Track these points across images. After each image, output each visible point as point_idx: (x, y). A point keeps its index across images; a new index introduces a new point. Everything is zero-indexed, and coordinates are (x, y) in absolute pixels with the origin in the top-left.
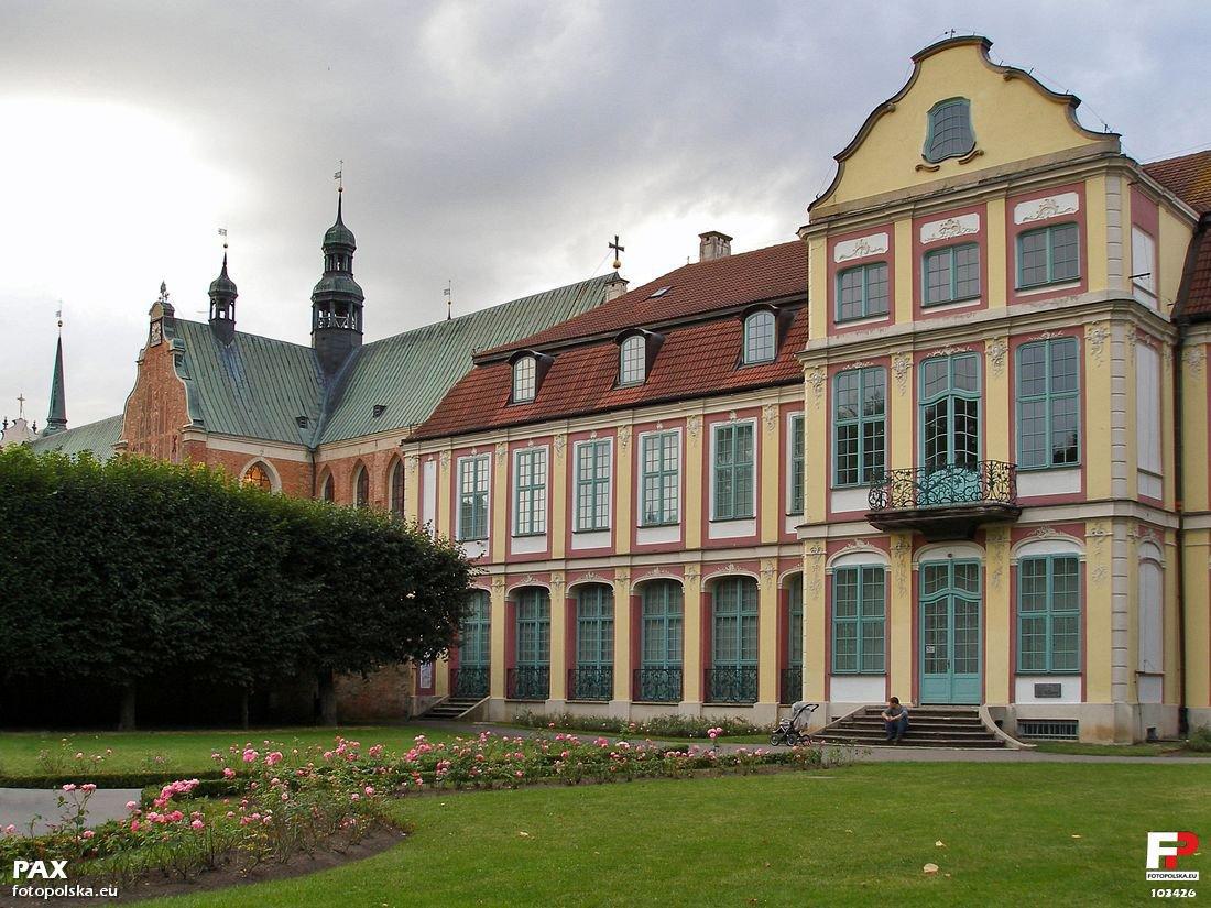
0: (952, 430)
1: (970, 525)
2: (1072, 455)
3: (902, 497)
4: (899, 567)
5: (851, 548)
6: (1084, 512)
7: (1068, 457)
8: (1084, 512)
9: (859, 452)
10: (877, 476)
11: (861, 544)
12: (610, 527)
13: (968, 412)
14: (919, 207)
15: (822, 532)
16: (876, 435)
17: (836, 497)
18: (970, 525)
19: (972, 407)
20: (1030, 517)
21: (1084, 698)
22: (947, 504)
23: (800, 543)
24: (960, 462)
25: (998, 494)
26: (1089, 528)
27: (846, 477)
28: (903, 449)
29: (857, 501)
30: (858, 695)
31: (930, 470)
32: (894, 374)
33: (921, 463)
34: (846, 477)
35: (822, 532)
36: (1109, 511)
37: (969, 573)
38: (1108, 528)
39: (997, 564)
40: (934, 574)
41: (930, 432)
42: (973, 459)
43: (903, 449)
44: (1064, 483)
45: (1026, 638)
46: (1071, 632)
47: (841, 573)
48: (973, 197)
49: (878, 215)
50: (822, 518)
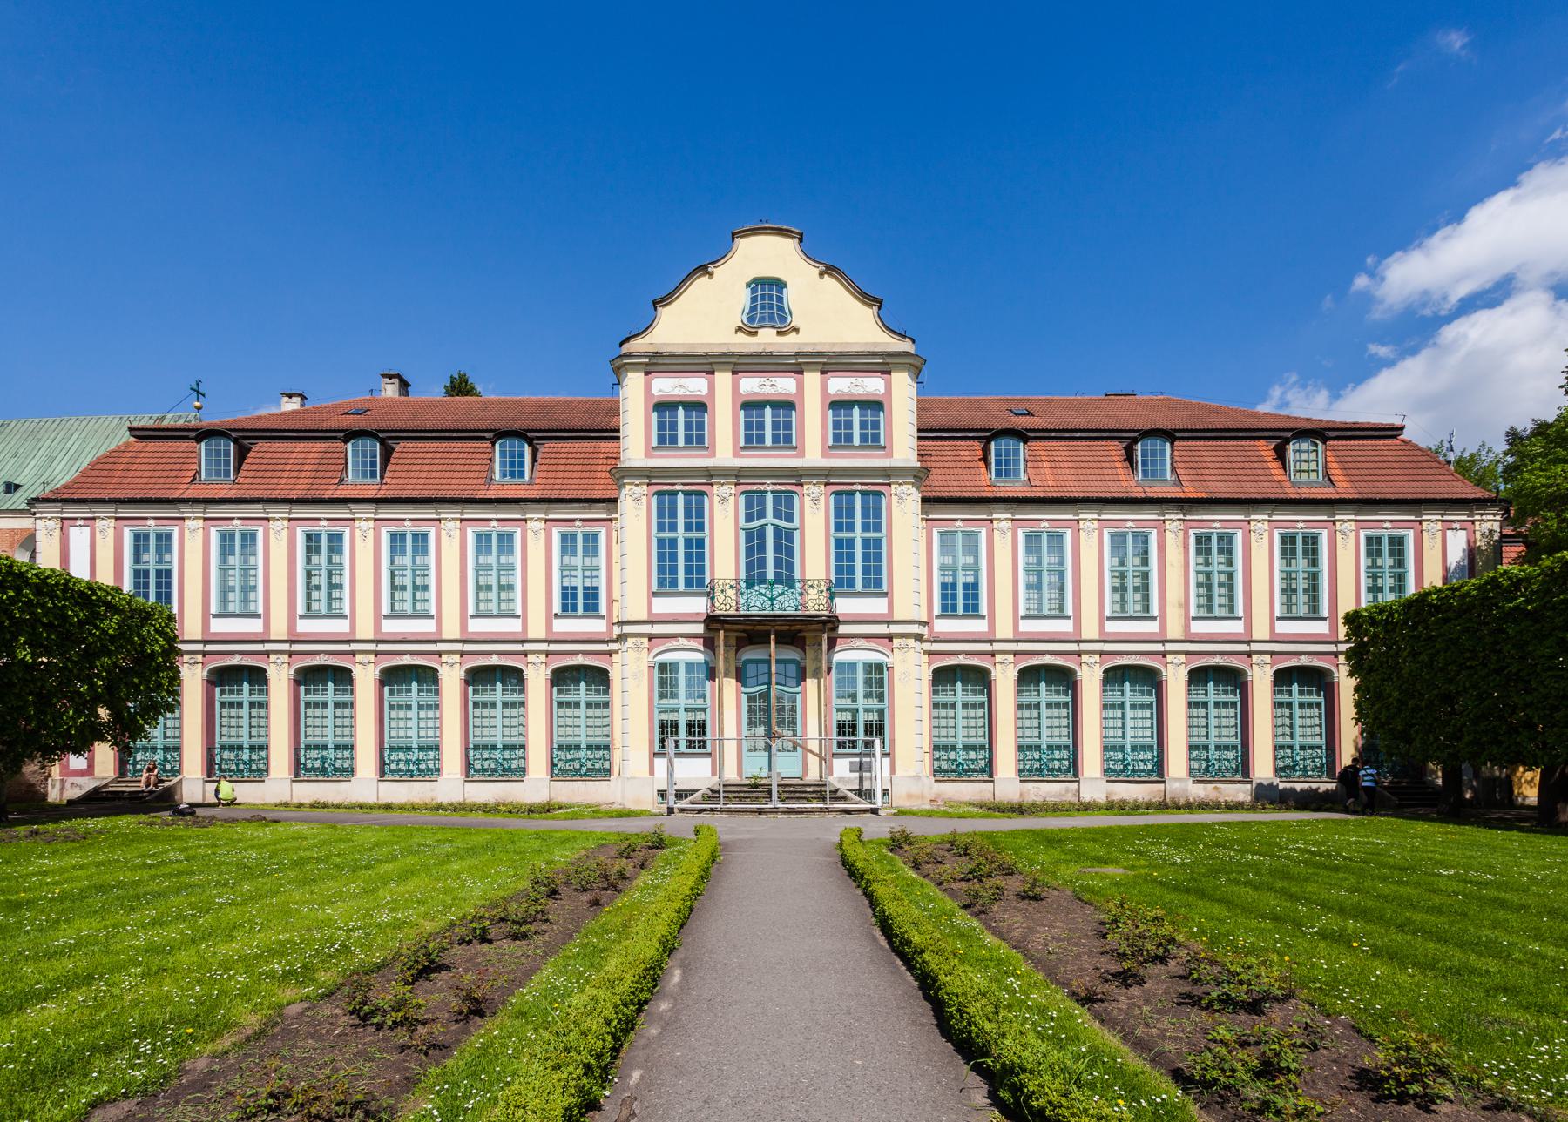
0: (770, 553)
2: (878, 583)
5: (674, 644)
6: (894, 629)
7: (875, 584)
8: (894, 629)
9: (680, 563)
10: (697, 582)
11: (683, 642)
12: (347, 611)
13: (785, 542)
15: (647, 629)
16: (697, 548)
17: (655, 600)
19: (789, 535)
20: (842, 629)
21: (652, 772)
22: (790, 611)
23: (622, 638)
24: (778, 579)
26: (896, 642)
27: (665, 584)
28: (725, 561)
29: (697, 605)
31: (750, 583)
32: (716, 499)
33: (743, 575)
34: (665, 584)
35: (647, 629)
36: (915, 629)
38: (911, 642)
41: (749, 551)
42: (790, 583)
43: (725, 561)
44: (876, 606)
47: (663, 667)
48: (796, 364)
49: (704, 363)
50: (644, 617)
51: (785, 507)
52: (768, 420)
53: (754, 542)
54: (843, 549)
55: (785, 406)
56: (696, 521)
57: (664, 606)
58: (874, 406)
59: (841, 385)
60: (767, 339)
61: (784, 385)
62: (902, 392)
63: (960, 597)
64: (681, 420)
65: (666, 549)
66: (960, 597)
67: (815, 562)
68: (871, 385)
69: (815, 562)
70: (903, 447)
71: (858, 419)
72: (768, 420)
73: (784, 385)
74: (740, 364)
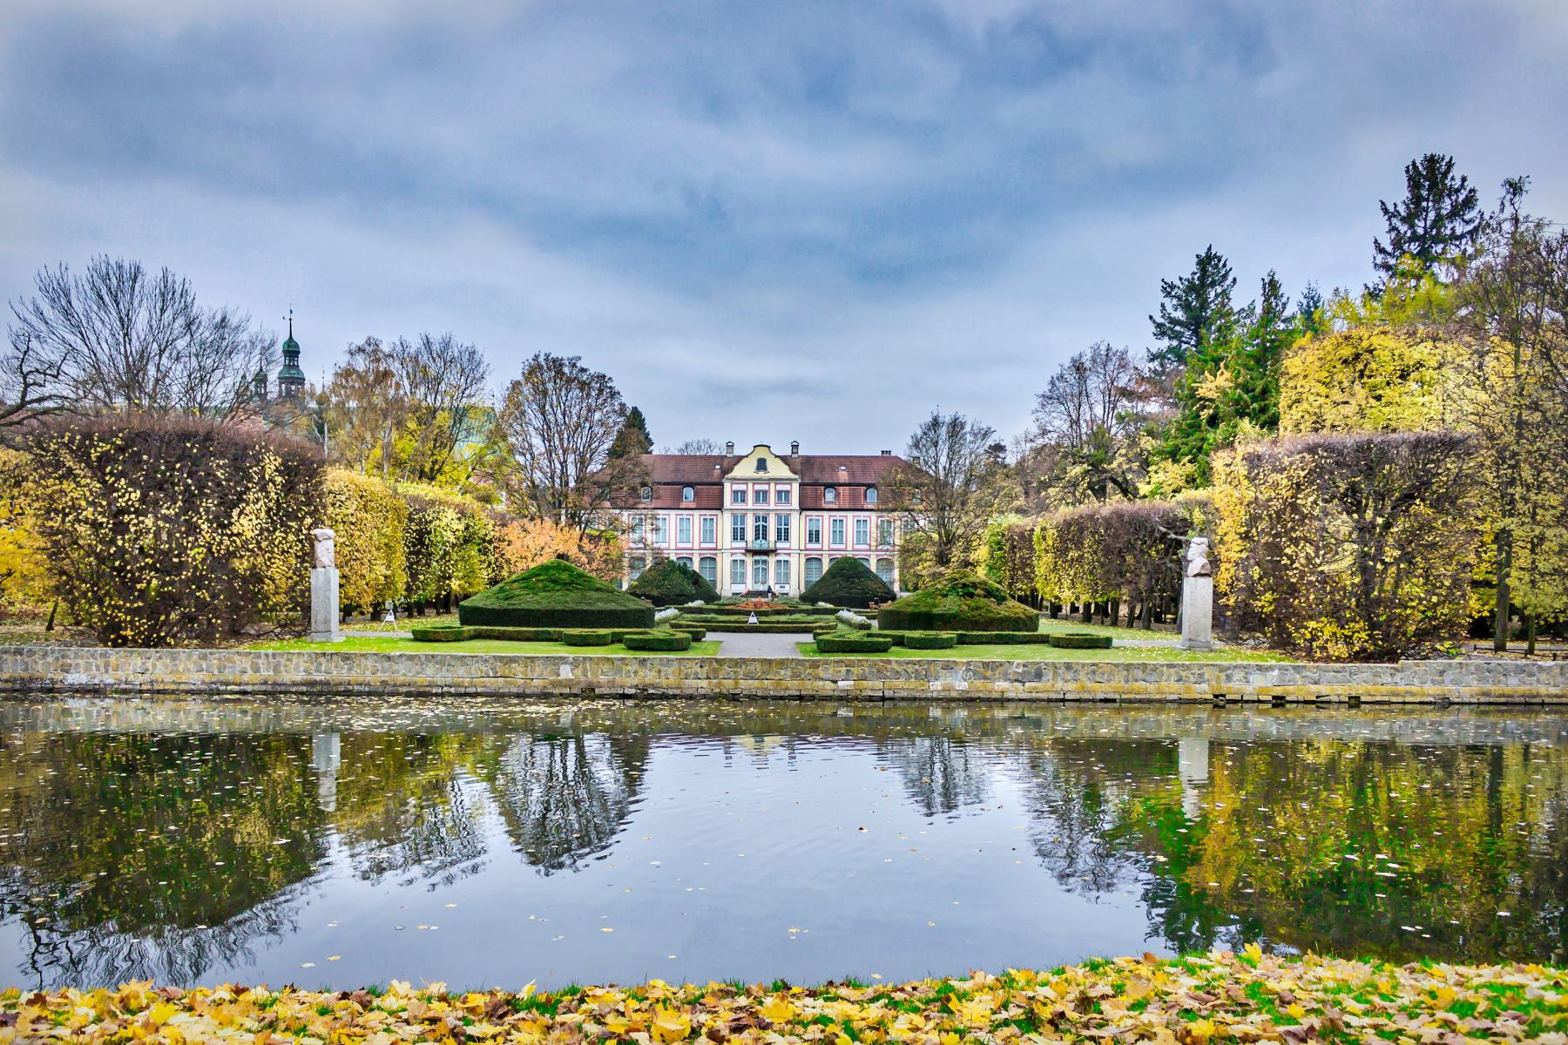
1: (767, 553)
3: (750, 546)
4: (749, 560)
13: (765, 528)
14: (755, 481)
18: (767, 553)
25: (772, 546)
27: (735, 538)
28: (750, 535)
29: (743, 544)
30: (741, 589)
37: (765, 562)
39: (772, 560)
40: (757, 562)
44: (786, 545)
45: (778, 574)
46: (787, 575)
49: (745, 480)
51: (765, 519)
52: (761, 496)
53: (757, 528)
54: (779, 531)
55: (765, 493)
56: (743, 522)
57: (736, 544)
58: (787, 493)
59: (780, 487)
60: (761, 474)
61: (765, 487)
62: (796, 488)
63: (814, 536)
64: (740, 496)
65: (735, 530)
66: (814, 536)
67: (772, 535)
68: (787, 487)
69: (772, 535)
70: (795, 503)
71: (783, 496)
72: (761, 496)
73: (765, 487)
74: (755, 481)
